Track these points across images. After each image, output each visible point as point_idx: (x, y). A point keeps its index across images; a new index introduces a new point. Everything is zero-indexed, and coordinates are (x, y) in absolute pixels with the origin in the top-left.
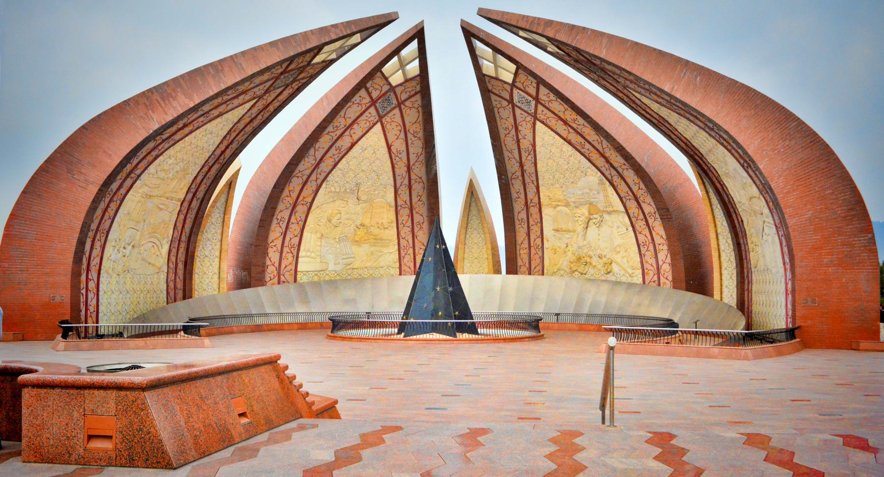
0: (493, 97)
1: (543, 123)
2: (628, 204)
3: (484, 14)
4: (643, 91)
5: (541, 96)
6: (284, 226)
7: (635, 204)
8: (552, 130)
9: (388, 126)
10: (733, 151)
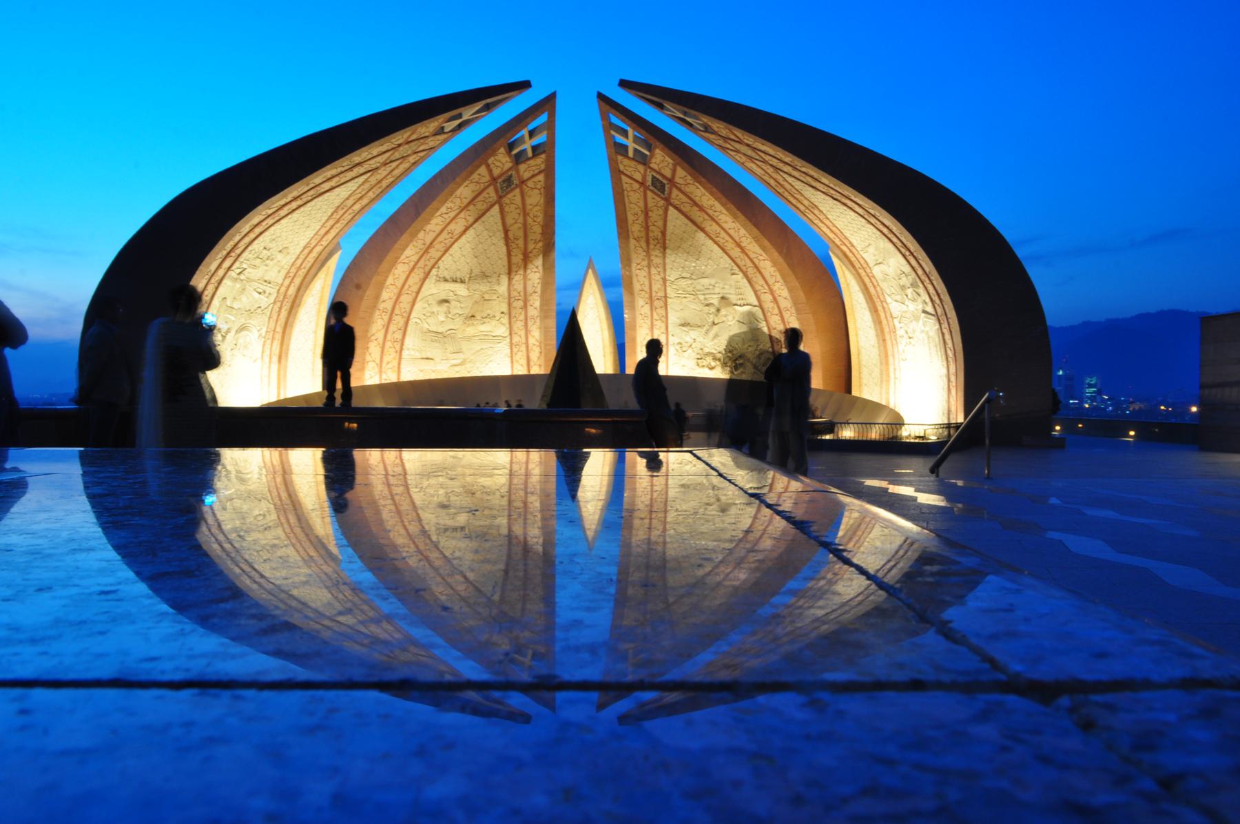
0: (624, 179)
1: (676, 208)
2: (763, 297)
3: (624, 84)
4: (796, 174)
6: (386, 318)
9: (507, 209)
10: (895, 240)
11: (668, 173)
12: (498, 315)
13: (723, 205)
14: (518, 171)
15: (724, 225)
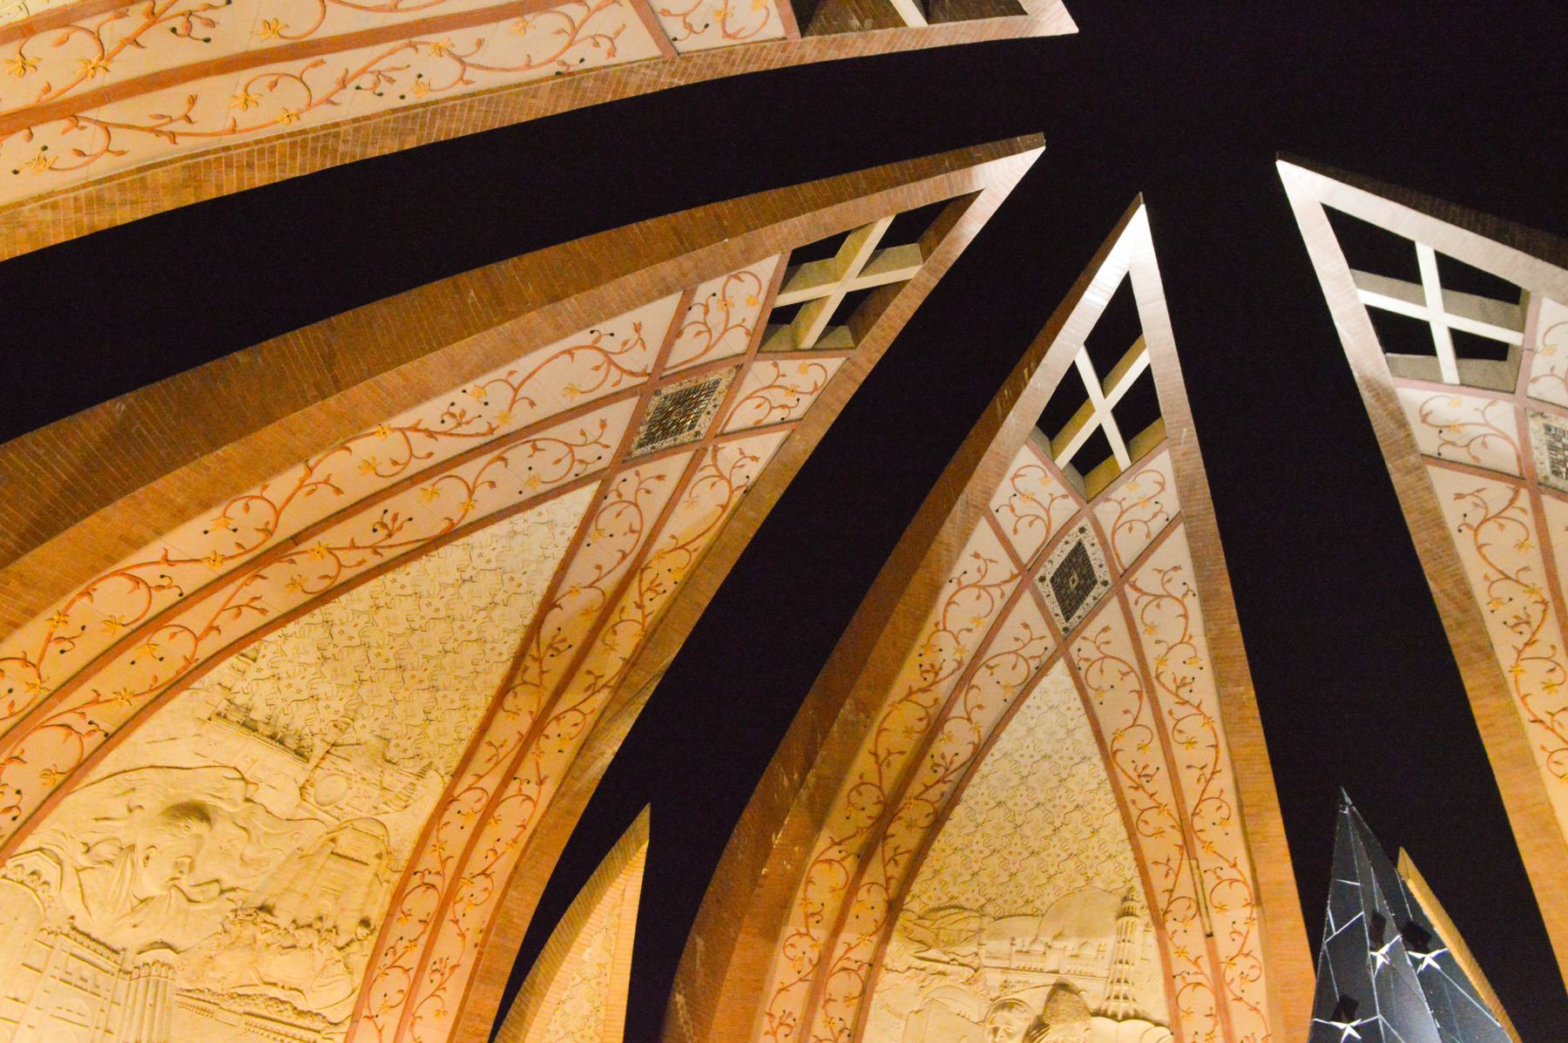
1: (1074, 670)
5: (1146, 578)
7: (1212, 1002)
8: (1086, 701)
9: (606, 519)
11: (1128, 547)
12: (349, 925)
13: (1221, 680)
14: (733, 387)
15: (1181, 754)
